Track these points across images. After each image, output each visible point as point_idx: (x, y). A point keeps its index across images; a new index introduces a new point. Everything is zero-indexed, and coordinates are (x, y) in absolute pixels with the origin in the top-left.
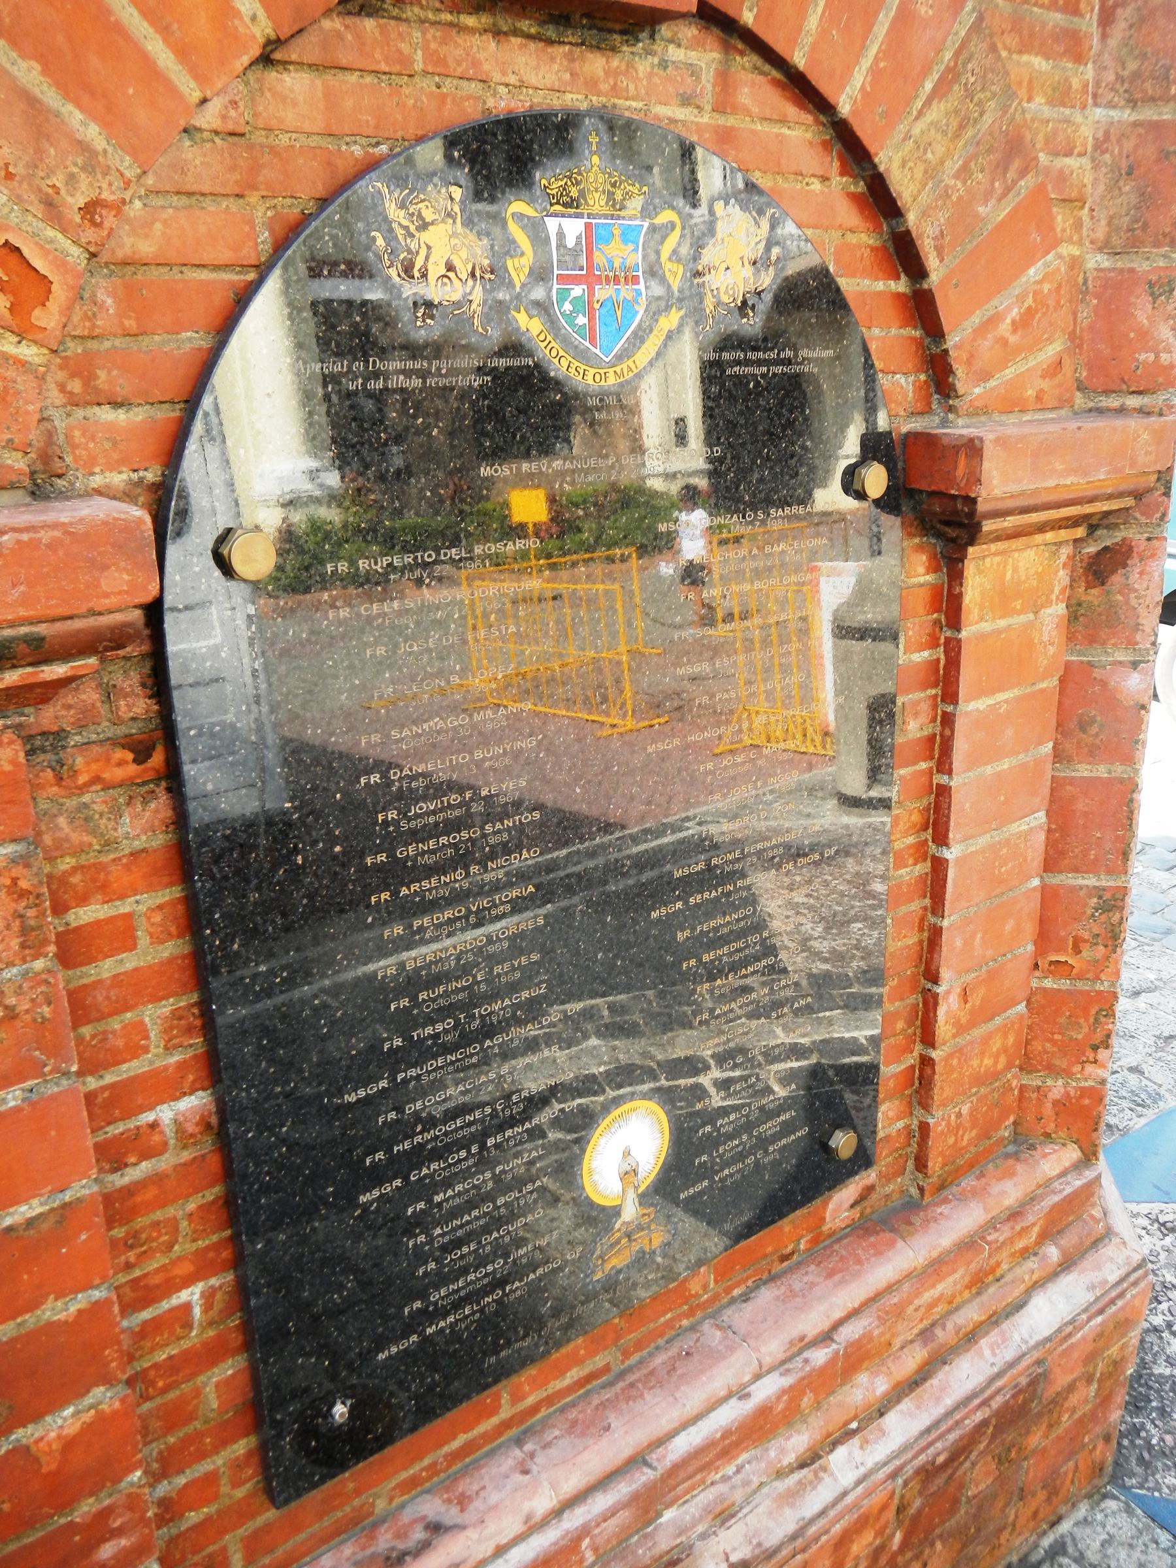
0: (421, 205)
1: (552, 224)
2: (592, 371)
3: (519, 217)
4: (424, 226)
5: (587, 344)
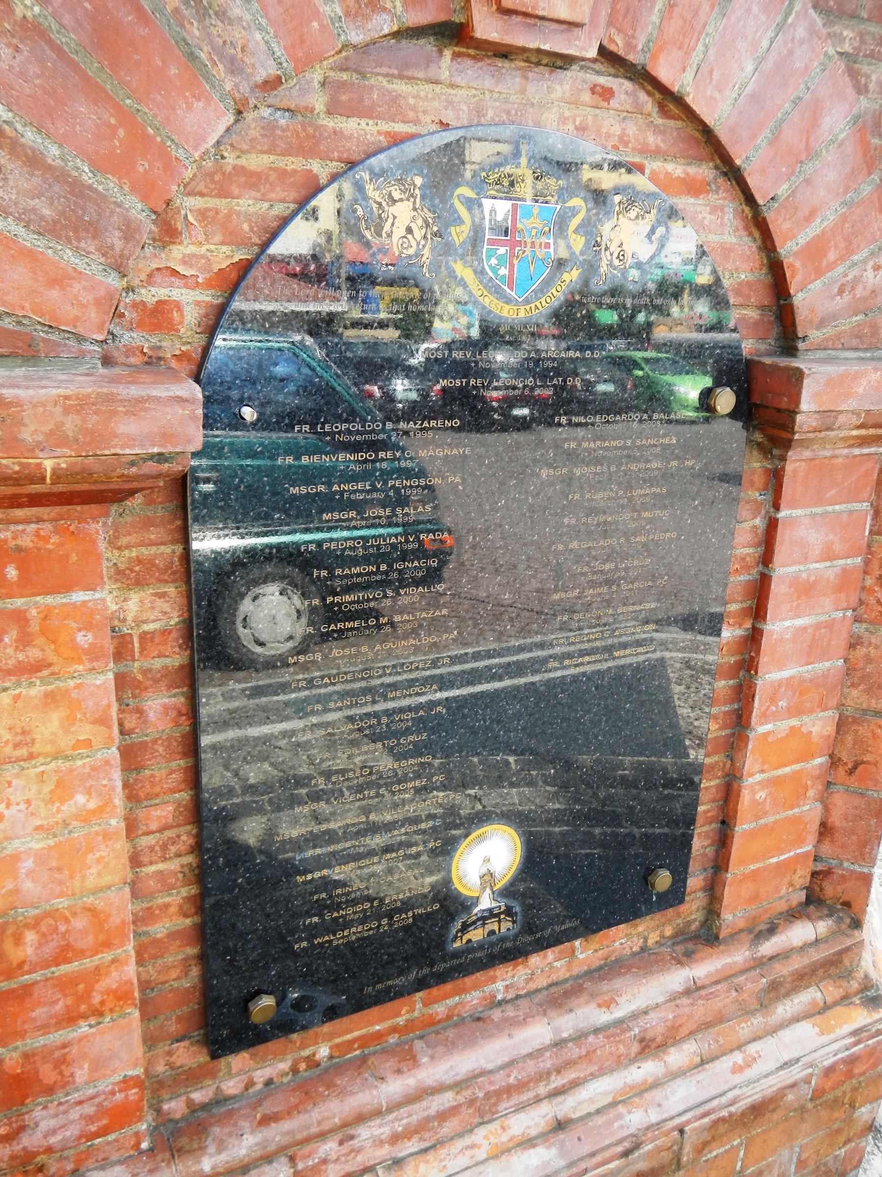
0: (392, 188)
1: (487, 203)
2: (507, 307)
5: (506, 288)
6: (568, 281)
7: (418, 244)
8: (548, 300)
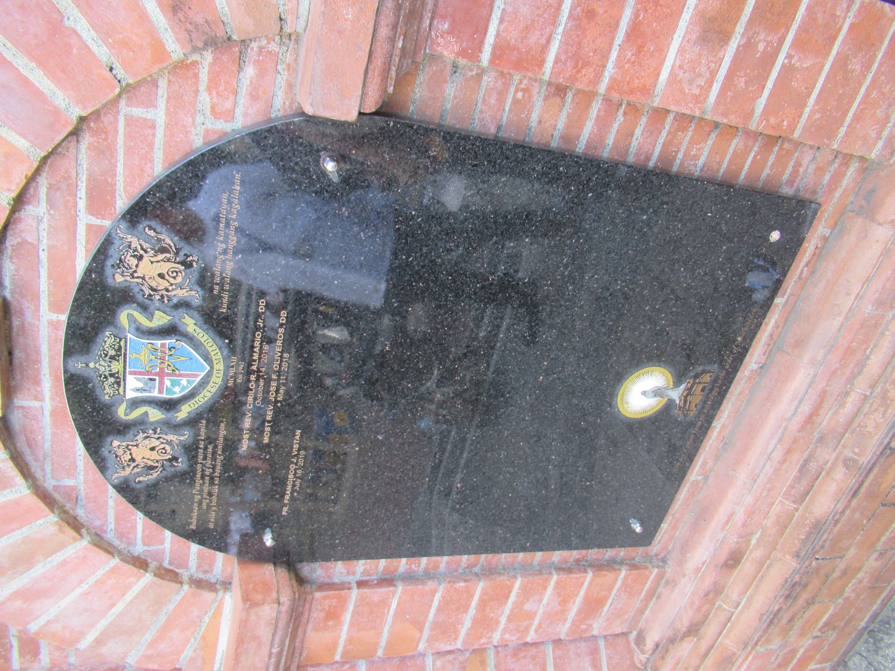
2: (214, 379)
3: (126, 415)
4: (133, 460)
6: (195, 327)
7: (162, 443)
8: (210, 344)
